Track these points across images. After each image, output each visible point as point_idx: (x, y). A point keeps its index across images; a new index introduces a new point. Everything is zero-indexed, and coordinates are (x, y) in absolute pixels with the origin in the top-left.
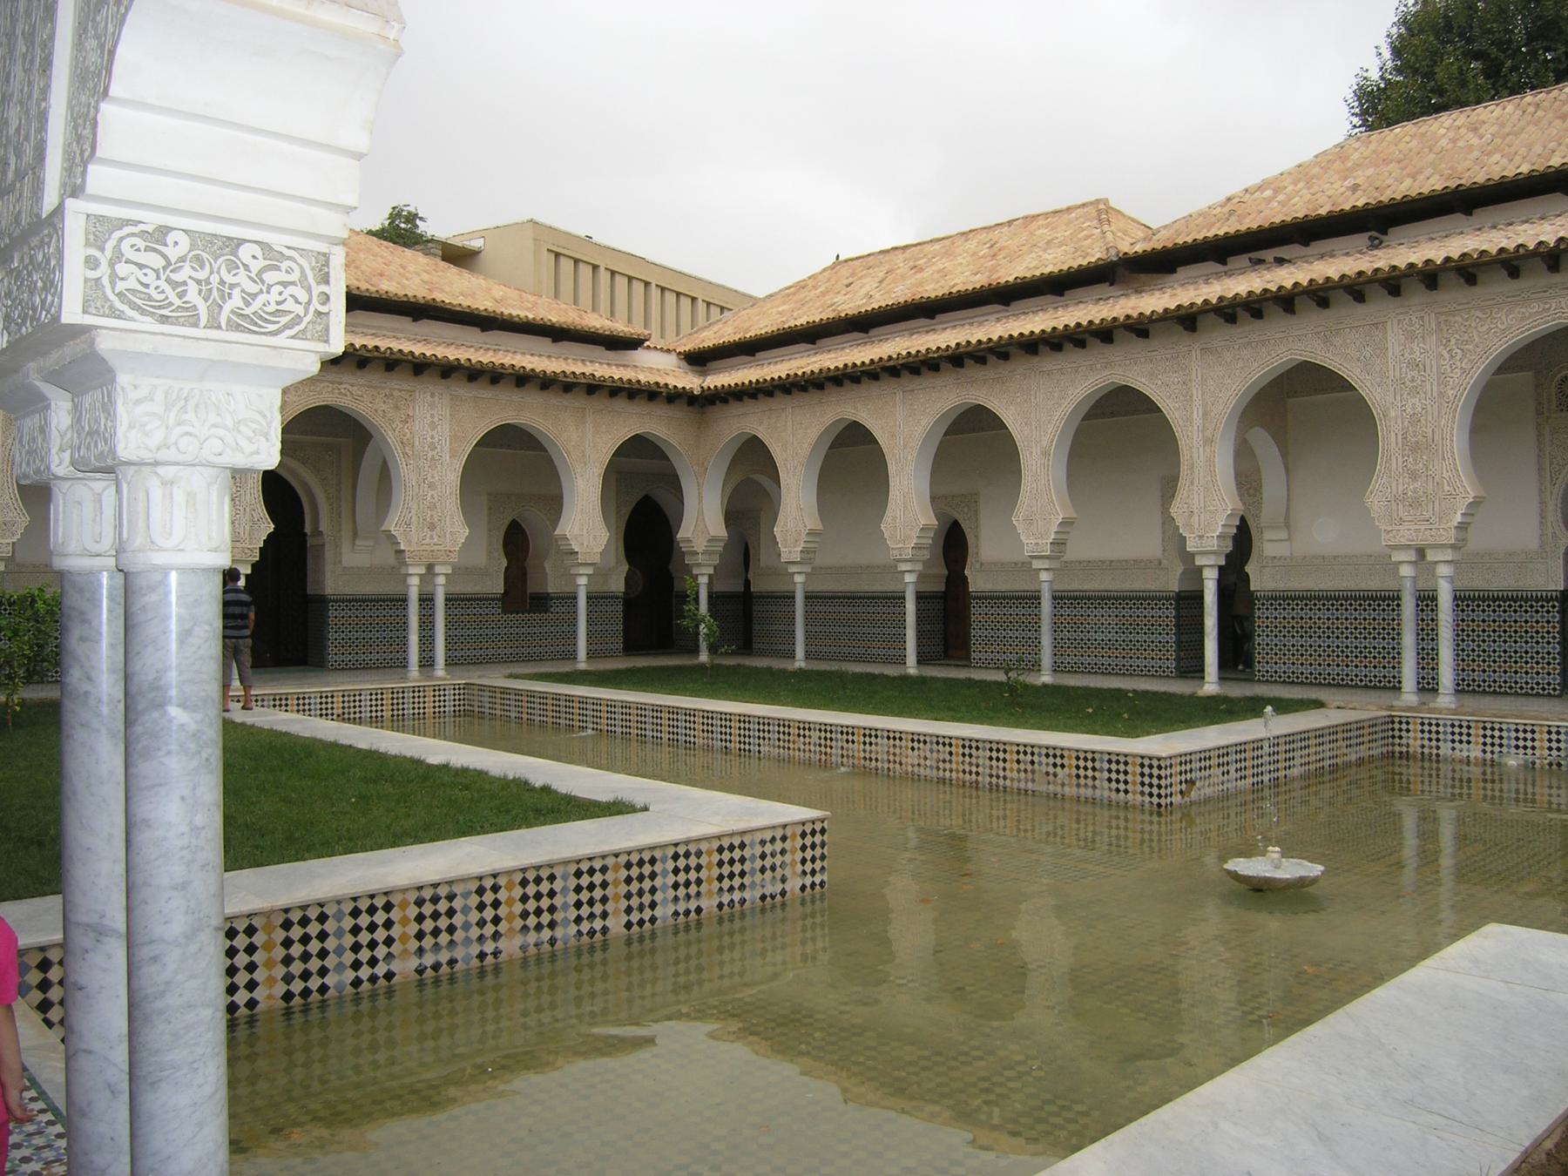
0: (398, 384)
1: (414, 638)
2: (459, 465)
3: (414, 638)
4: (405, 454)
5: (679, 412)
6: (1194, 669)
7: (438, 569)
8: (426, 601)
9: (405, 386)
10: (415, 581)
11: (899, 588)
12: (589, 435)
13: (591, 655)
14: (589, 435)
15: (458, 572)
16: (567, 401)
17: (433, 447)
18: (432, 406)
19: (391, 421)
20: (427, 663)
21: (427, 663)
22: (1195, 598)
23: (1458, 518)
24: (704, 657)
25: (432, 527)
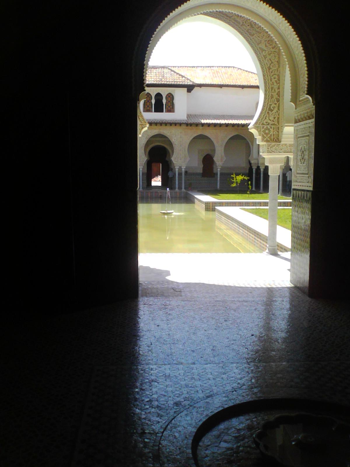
7: (182, 167)
8: (180, 174)
20: (180, 188)
21: (180, 188)
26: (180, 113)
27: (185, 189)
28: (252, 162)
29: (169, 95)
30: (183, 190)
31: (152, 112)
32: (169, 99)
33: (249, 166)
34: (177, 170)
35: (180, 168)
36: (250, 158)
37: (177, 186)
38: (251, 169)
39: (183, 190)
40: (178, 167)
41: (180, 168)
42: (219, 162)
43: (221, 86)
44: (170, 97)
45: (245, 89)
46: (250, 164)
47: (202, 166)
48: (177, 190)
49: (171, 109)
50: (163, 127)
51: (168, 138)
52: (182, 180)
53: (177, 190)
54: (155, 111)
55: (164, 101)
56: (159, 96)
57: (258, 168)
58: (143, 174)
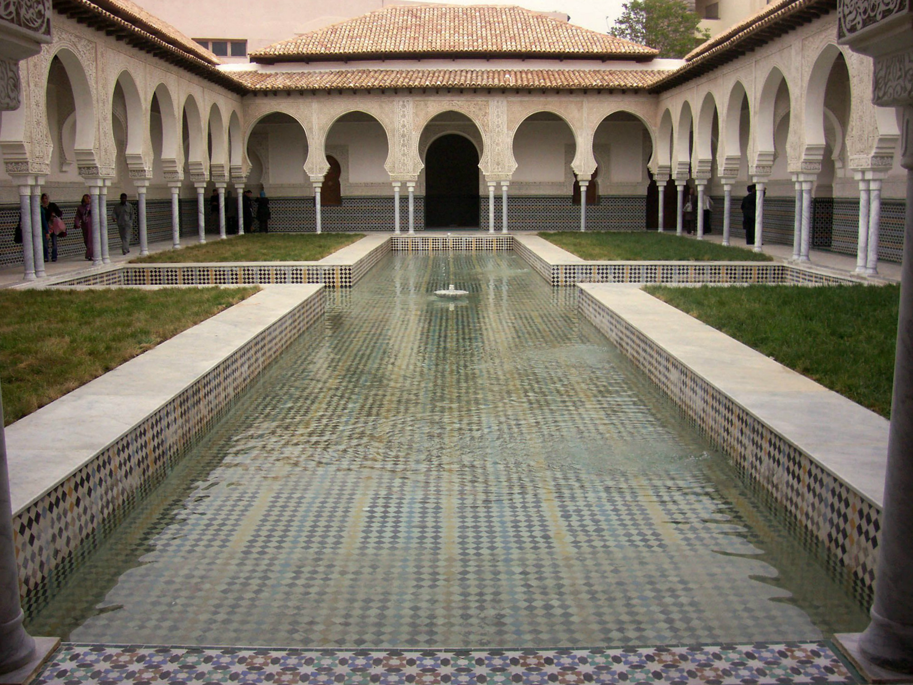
0: (480, 100)
1: (492, 215)
2: (512, 134)
3: (492, 215)
4: (485, 131)
5: (641, 99)
6: (751, 240)
8: (498, 199)
9: (484, 99)
10: (492, 189)
11: (791, 195)
12: (585, 115)
13: (586, 227)
14: (585, 115)
15: (512, 184)
16: (573, 99)
17: (498, 126)
18: (497, 107)
19: (477, 116)
22: (855, 203)
23: (803, 157)
24: (660, 230)
25: (498, 164)
27: (510, 228)
28: (654, 171)
30: (505, 231)
33: (649, 182)
34: (492, 189)
35: (498, 186)
36: (649, 165)
38: (653, 188)
39: (505, 231)
41: (498, 186)
46: (651, 175)
48: (492, 231)
51: (469, 120)
53: (492, 231)
57: (671, 185)
58: (415, 198)
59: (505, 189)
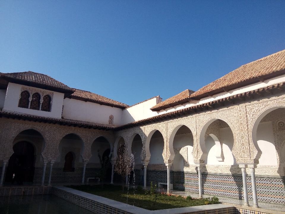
20: (46, 182)
26: (55, 113)
29: (47, 97)
30: (50, 185)
31: (27, 108)
32: (46, 100)
35: (49, 163)
37: (43, 181)
40: (47, 162)
41: (49, 163)
42: (86, 158)
43: (86, 100)
44: (48, 99)
45: (103, 106)
47: (65, 161)
49: (47, 107)
50: (37, 123)
52: (46, 174)
54: (30, 108)
55: (42, 101)
56: (37, 96)
59: (52, 165)
